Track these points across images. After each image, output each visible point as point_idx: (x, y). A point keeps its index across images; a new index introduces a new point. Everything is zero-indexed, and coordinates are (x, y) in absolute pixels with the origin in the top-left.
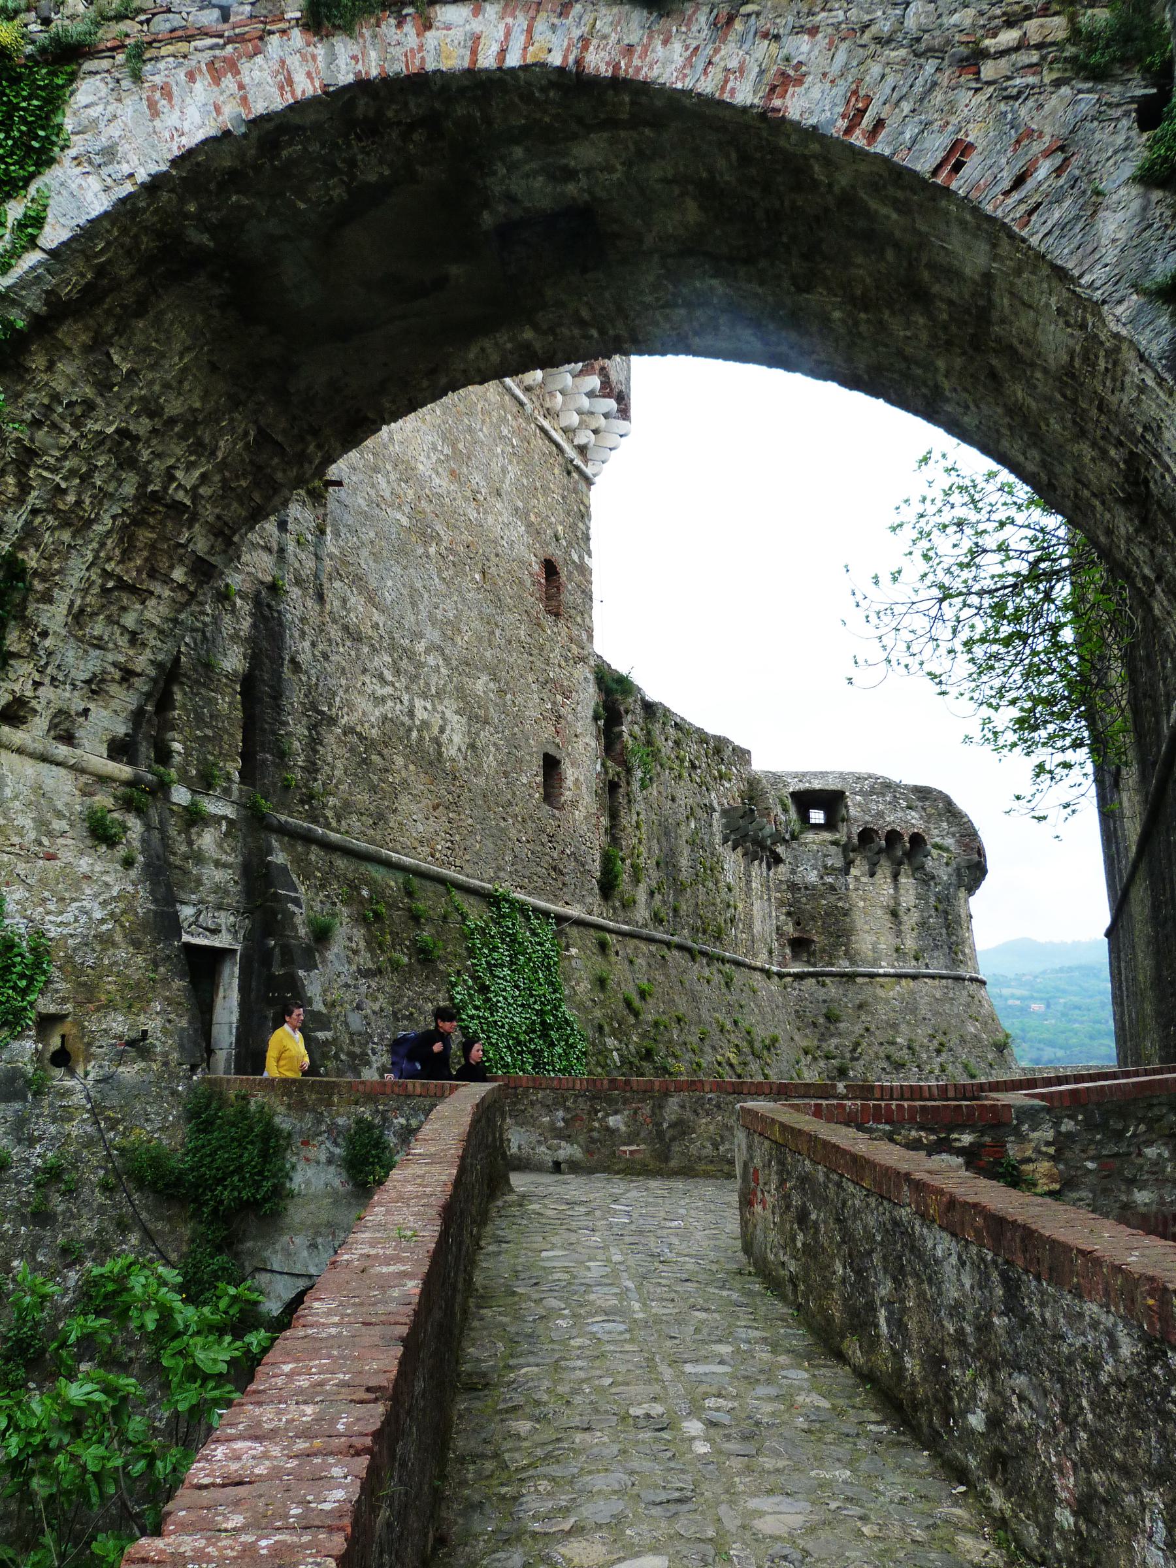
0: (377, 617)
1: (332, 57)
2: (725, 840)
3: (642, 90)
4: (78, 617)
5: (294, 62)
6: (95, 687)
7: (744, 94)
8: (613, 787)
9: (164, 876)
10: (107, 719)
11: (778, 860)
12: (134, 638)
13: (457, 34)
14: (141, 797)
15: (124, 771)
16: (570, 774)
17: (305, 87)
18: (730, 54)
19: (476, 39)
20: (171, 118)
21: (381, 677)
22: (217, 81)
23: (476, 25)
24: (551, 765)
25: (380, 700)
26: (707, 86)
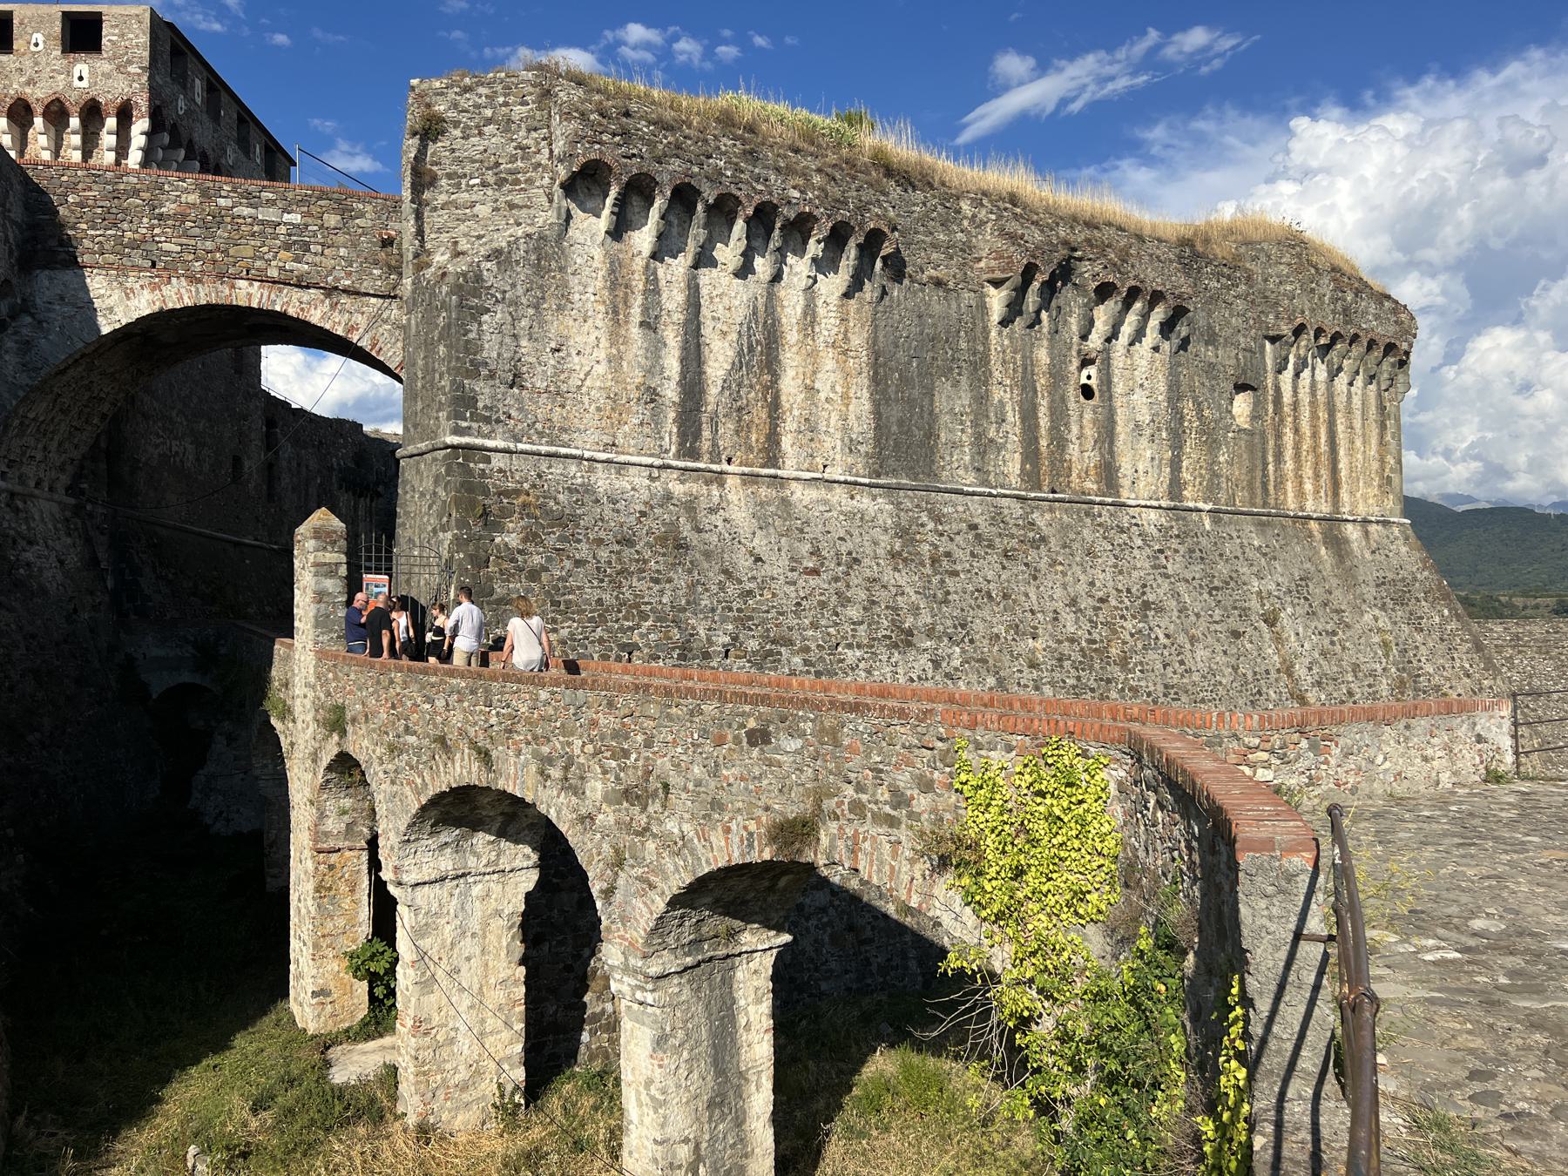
0: (155, 404)
1: (197, 291)
2: (340, 487)
3: (308, 324)
4: (60, 445)
5: (183, 291)
6: (62, 469)
7: (340, 331)
8: (270, 466)
9: (88, 541)
10: (65, 479)
11: (379, 495)
12: (76, 447)
13: (243, 292)
14: (78, 510)
15: (72, 501)
16: (247, 464)
17: (188, 302)
18: (336, 317)
19: (250, 295)
20: (133, 303)
21: (158, 436)
22: (153, 290)
23: (251, 290)
24: (237, 462)
25: (157, 446)
26: (327, 327)
